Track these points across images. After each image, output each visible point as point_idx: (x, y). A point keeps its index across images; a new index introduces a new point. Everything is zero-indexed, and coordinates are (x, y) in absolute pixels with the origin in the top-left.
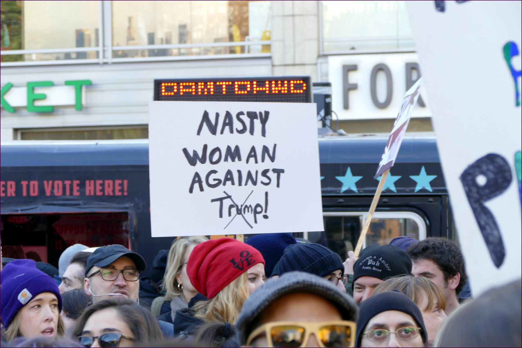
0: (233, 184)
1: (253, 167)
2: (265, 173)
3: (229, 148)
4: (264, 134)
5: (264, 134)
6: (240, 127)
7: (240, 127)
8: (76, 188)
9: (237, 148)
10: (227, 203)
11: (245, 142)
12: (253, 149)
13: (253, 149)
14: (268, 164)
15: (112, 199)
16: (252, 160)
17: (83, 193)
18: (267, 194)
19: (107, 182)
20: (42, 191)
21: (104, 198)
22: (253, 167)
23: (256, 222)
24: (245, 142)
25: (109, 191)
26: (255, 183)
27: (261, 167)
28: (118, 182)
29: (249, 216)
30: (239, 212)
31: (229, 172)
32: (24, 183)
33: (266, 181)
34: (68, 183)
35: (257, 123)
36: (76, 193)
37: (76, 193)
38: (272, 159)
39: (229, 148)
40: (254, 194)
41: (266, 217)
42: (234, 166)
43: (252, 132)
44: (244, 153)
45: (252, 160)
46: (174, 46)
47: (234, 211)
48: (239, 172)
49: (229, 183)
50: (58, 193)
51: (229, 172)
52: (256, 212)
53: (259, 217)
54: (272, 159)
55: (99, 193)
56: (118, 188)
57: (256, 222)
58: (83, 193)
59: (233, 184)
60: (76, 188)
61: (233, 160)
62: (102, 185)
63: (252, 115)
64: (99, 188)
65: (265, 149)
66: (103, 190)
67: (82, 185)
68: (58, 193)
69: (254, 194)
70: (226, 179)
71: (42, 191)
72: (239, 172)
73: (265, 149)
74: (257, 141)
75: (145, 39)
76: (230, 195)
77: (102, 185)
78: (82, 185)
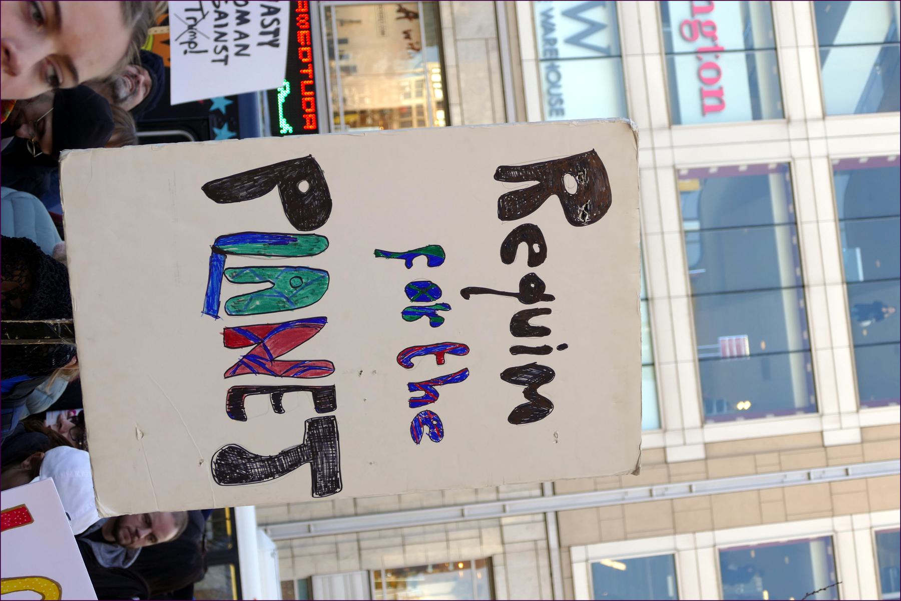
0: (216, 20)
1: (231, 37)
2: (225, 48)
3: (247, 13)
4: (260, 44)
5: (260, 44)
6: (266, 23)
7: (266, 23)
9: (247, 21)
10: (198, 15)
11: (253, 28)
12: (246, 36)
13: (246, 36)
14: (233, 50)
16: (237, 36)
18: (206, 51)
22: (231, 37)
23: (182, 43)
24: (253, 28)
26: (216, 40)
27: (231, 44)
29: (187, 37)
30: (191, 27)
31: (226, 15)
33: (218, 50)
35: (270, 38)
38: (237, 54)
39: (247, 13)
40: (205, 41)
41: (185, 52)
42: (232, 19)
43: (262, 33)
44: (244, 28)
45: (237, 36)
46: (337, 63)
47: (191, 22)
48: (226, 25)
49: (216, 15)
51: (226, 15)
52: (190, 43)
53: (186, 47)
54: (237, 54)
57: (182, 43)
59: (216, 20)
61: (238, 18)
63: (276, 33)
65: (246, 47)
69: (205, 41)
70: (220, 13)
72: (226, 25)
73: (246, 47)
74: (253, 40)
75: (342, 36)
76: (207, 17)
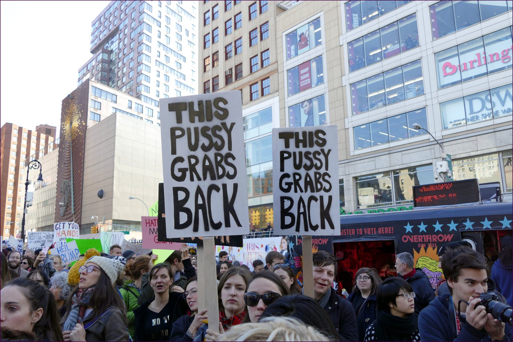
8: (375, 231)
15: (388, 235)
17: (377, 233)
19: (386, 228)
20: (364, 232)
21: (388, 235)
25: (386, 232)
28: (390, 228)
32: (358, 230)
34: (372, 229)
36: (375, 233)
37: (375, 233)
50: (369, 233)
55: (383, 233)
56: (390, 230)
58: (377, 233)
60: (375, 231)
62: (384, 229)
64: (383, 230)
66: (384, 231)
67: (377, 230)
68: (369, 233)
71: (364, 232)
77: (384, 229)
78: (377, 230)
